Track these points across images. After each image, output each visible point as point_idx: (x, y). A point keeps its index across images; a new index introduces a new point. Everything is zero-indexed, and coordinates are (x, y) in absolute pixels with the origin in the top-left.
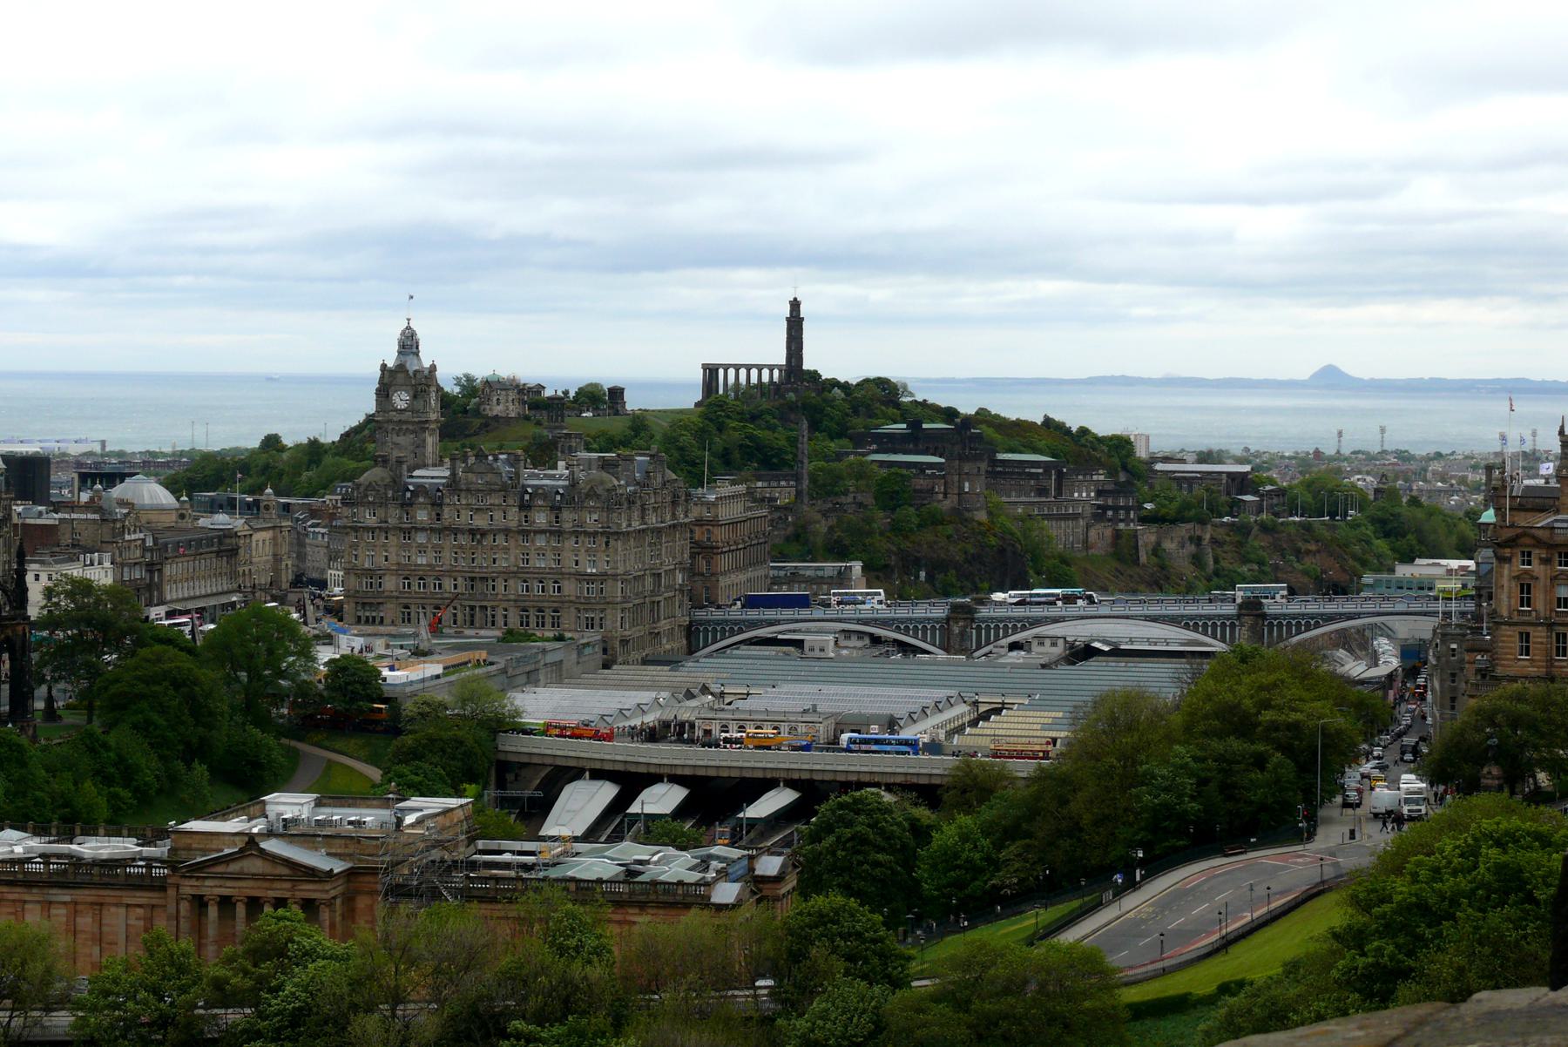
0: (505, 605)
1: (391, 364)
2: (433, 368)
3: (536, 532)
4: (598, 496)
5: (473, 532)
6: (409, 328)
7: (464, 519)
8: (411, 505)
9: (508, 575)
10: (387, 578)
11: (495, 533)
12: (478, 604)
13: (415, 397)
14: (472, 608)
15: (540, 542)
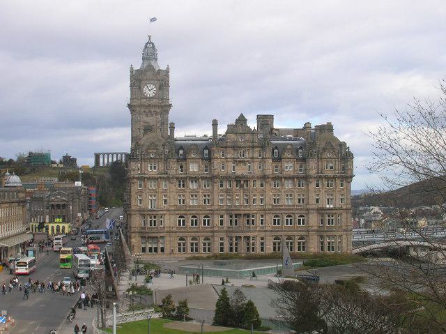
0: (263, 235)
1: (137, 67)
2: (167, 72)
3: (285, 178)
4: (332, 148)
5: (238, 179)
6: (150, 42)
7: (230, 169)
8: (185, 159)
9: (264, 211)
10: (167, 217)
11: (254, 179)
12: (243, 235)
13: (160, 88)
14: (238, 238)
15: (288, 185)
